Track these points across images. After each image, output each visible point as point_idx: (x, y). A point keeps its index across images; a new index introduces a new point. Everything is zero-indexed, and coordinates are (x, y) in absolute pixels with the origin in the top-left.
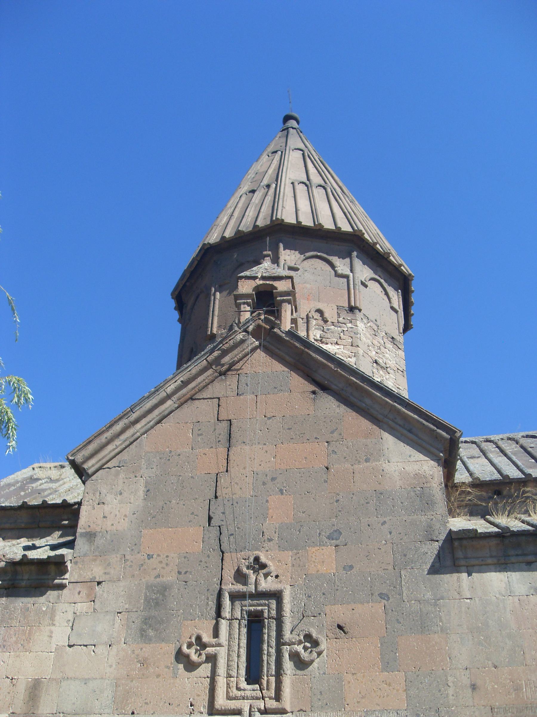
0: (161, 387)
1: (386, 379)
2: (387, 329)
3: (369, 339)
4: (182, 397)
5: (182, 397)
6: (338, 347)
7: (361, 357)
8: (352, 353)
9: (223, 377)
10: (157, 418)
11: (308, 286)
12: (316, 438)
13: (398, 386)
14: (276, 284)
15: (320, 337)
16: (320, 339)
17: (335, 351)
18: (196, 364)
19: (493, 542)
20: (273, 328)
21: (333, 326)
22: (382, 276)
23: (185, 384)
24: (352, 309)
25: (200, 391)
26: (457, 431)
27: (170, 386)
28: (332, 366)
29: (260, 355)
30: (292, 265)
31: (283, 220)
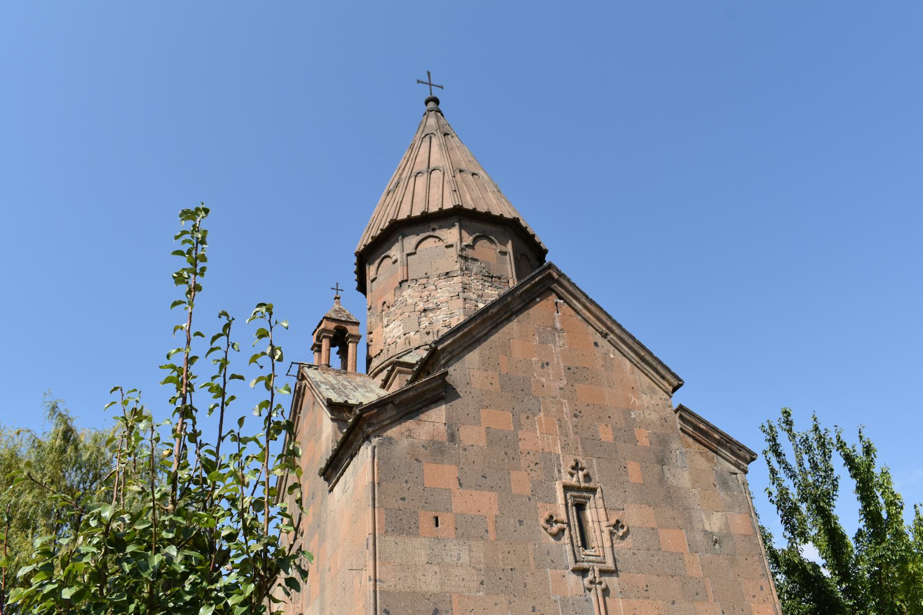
1: (436, 316)
2: (438, 272)
6: (394, 323)
11: (381, 286)
13: (451, 312)
19: (330, 469)
22: (436, 226)
24: (400, 283)
30: (373, 277)
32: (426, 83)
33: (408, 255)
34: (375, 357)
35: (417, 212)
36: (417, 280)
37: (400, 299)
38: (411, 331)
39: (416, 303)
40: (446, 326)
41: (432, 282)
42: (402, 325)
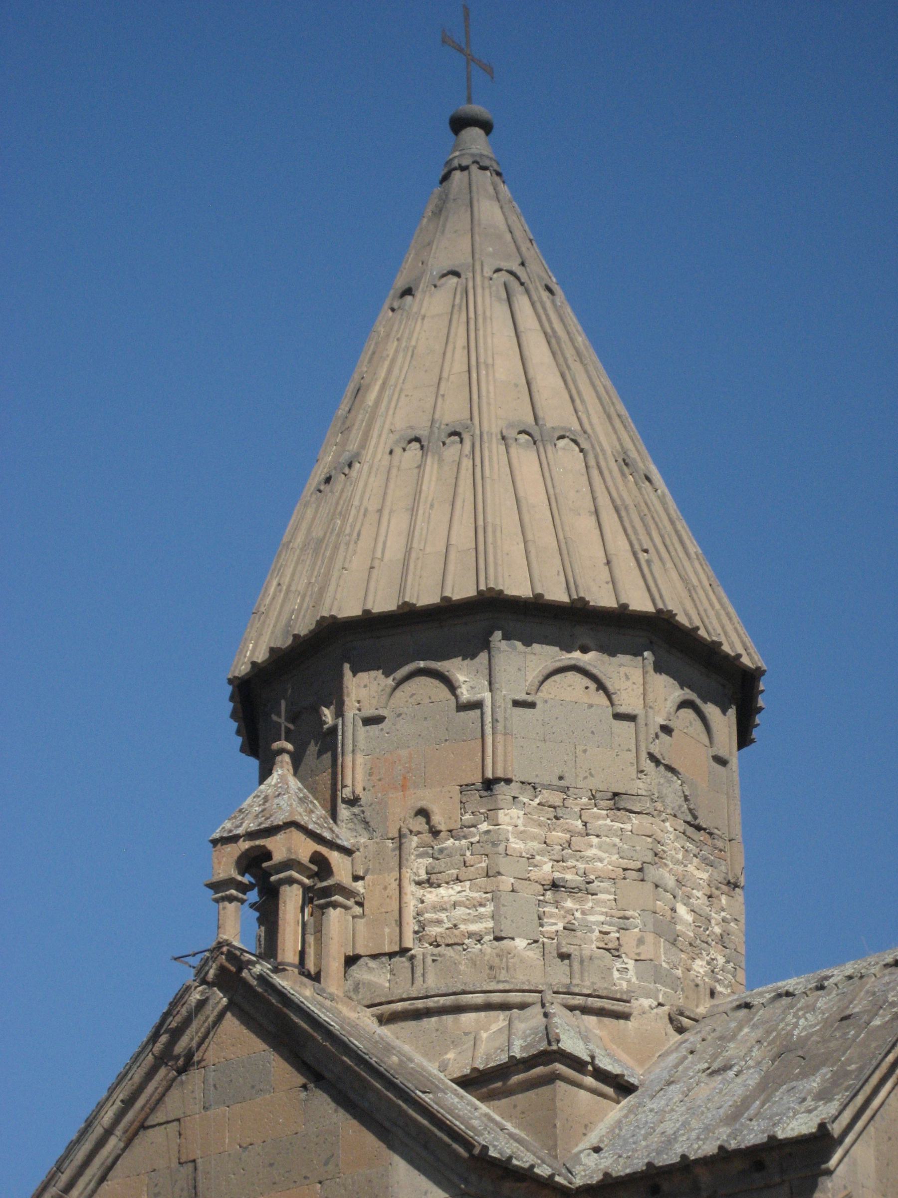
0: (94, 1118)
2: (595, 783)
3: (534, 838)
4: (130, 1127)
5: (130, 1127)
6: (458, 888)
7: (507, 898)
8: (486, 893)
9: (183, 1077)
10: (99, 1174)
11: (403, 753)
12: (306, 1178)
13: (621, 914)
14: (269, 843)
15: (427, 873)
16: (424, 877)
17: (453, 899)
18: (138, 1064)
20: (240, 970)
21: (452, 840)
23: (129, 1103)
24: (489, 784)
25: (153, 1110)
26: (476, 1143)
27: (107, 1112)
28: (319, 1038)
29: (231, 1022)
30: (369, 712)
31: (333, 617)
32: (461, 50)
33: (516, 703)
34: (374, 957)
35: (557, 594)
36: (535, 788)
37: (484, 827)
38: (519, 937)
39: (533, 857)
40: (608, 950)
41: (577, 809)
42: (489, 909)
